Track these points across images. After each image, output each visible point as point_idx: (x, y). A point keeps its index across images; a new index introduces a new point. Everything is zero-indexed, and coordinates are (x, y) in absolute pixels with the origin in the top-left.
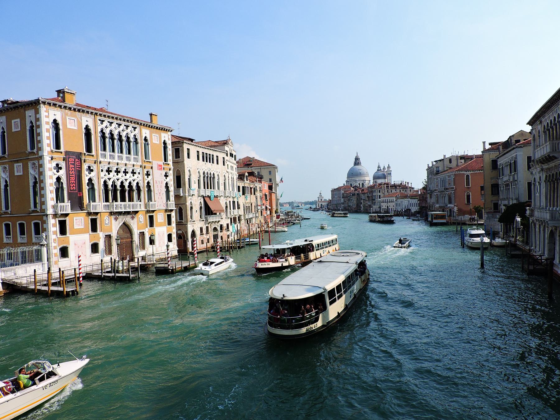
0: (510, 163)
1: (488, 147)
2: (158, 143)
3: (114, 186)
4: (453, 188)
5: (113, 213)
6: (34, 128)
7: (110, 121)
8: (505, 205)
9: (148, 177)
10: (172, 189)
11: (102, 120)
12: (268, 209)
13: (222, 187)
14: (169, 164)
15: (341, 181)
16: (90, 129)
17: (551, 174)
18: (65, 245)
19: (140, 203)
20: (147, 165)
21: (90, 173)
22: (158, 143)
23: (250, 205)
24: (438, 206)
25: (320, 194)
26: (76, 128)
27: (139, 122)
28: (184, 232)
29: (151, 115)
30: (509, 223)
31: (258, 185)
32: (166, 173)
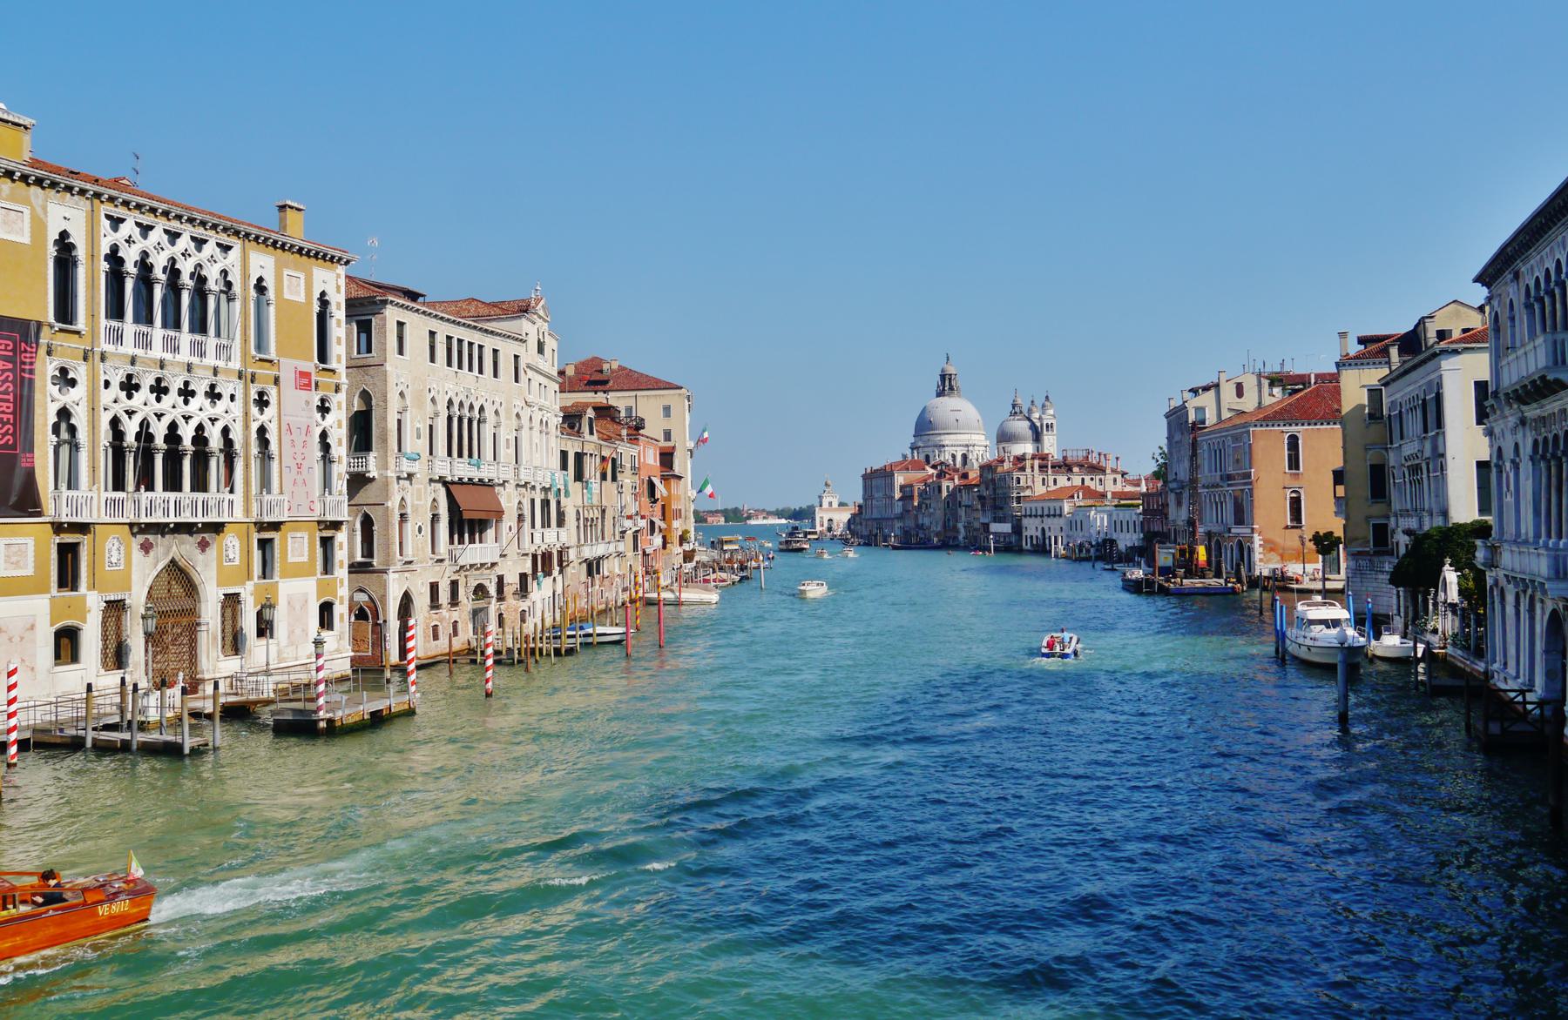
0: (1424, 400)
1: (1354, 348)
2: (301, 298)
3: (145, 435)
5: (135, 530)
7: (145, 223)
8: (1408, 532)
9: (262, 412)
11: (115, 215)
12: (657, 530)
13: (506, 453)
14: (333, 371)
16: (71, 247)
17: (1550, 437)
19: (231, 497)
20: (264, 371)
22: (301, 298)
23: (597, 514)
25: (826, 484)
26: (25, 239)
27: (242, 228)
28: (375, 596)
29: (283, 208)
30: (1422, 589)
31: (626, 451)
32: (323, 401)
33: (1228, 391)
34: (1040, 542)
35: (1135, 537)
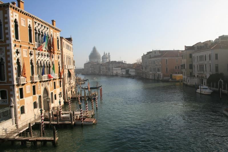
0: (205, 56)
6: (2, 24)
7: (39, 23)
10: (61, 65)
11: (35, 21)
14: (59, 51)
15: (87, 59)
18: (22, 105)
21: (31, 56)
26: (25, 26)
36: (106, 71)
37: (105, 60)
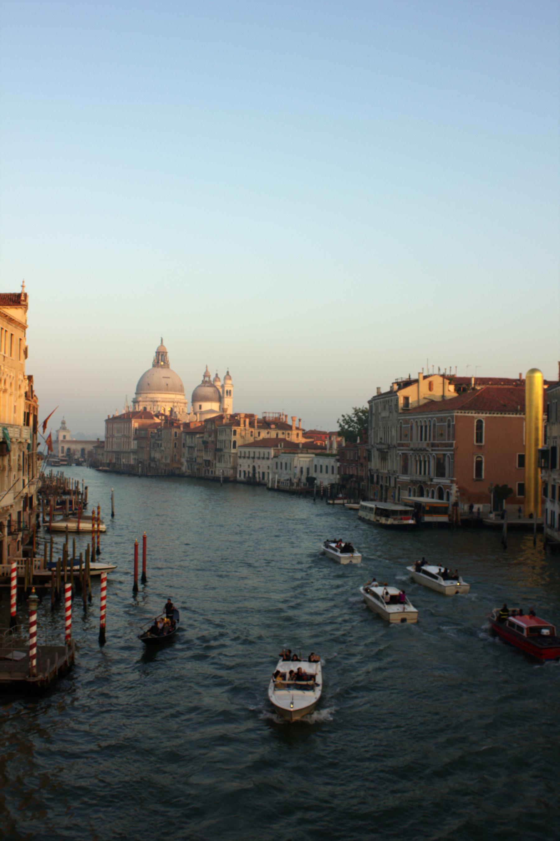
4: (451, 445)
24: (409, 478)
33: (424, 384)
34: (251, 475)
35: (332, 477)
36: (206, 461)
37: (207, 406)
